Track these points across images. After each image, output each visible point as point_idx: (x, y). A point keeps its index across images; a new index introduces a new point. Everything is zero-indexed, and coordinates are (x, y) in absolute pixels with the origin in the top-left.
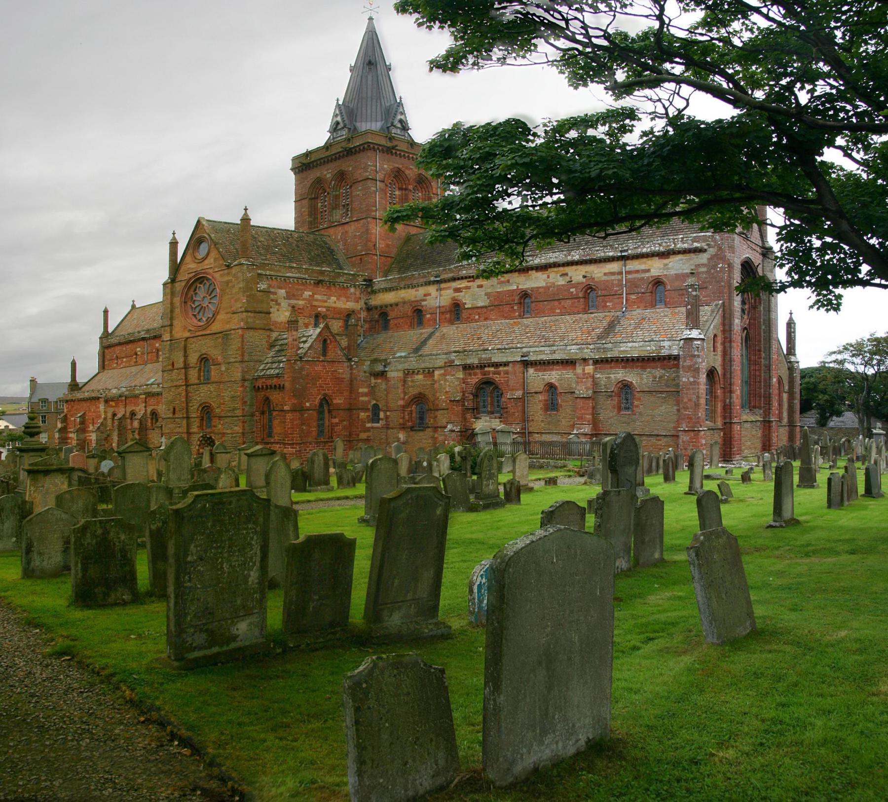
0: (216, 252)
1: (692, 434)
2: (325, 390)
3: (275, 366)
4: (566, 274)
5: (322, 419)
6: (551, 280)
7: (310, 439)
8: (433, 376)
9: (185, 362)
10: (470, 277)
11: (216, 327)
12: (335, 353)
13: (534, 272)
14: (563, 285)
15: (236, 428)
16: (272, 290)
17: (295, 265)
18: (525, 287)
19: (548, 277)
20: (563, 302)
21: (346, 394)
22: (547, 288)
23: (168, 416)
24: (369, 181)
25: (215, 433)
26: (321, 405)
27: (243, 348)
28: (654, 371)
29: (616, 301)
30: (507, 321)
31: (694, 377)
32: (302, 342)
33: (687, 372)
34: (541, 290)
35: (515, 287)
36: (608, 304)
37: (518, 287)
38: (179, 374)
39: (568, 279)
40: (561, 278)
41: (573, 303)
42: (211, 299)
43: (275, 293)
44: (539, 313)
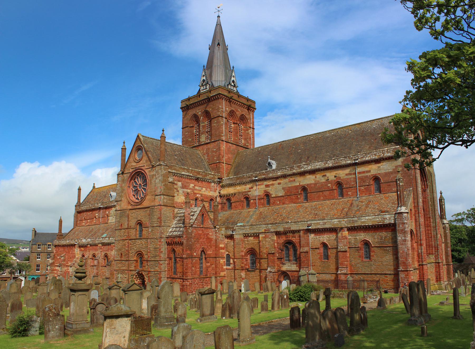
0: (146, 156)
1: (406, 273)
2: (203, 245)
3: (178, 229)
4: (325, 175)
5: (202, 263)
6: (317, 179)
7: (196, 276)
8: (259, 238)
9: (128, 224)
10: (274, 178)
11: (146, 204)
12: (209, 223)
13: (308, 174)
14: (324, 182)
15: (157, 268)
16: (175, 182)
17: (186, 168)
18: (304, 183)
19: (316, 177)
20: (324, 192)
21: (214, 248)
22: (315, 184)
23: (118, 259)
24: (220, 118)
25: (145, 271)
26: (201, 255)
27: (161, 218)
28: (381, 234)
29: (353, 191)
30: (295, 205)
31: (405, 237)
32: (191, 215)
33: (401, 234)
34: (313, 185)
35: (298, 184)
36: (349, 193)
37: (300, 184)
38: (125, 232)
39: (326, 178)
40: (323, 178)
41: (330, 193)
42: (143, 186)
43: (176, 184)
44: (313, 200)
